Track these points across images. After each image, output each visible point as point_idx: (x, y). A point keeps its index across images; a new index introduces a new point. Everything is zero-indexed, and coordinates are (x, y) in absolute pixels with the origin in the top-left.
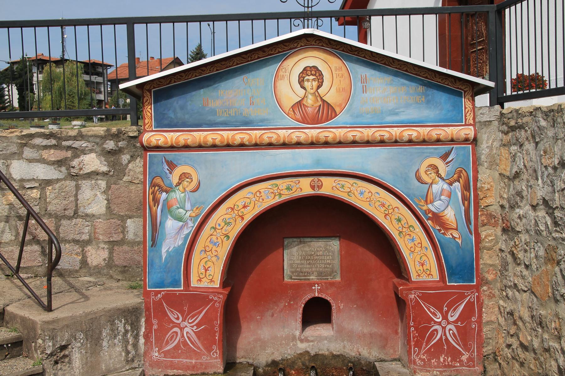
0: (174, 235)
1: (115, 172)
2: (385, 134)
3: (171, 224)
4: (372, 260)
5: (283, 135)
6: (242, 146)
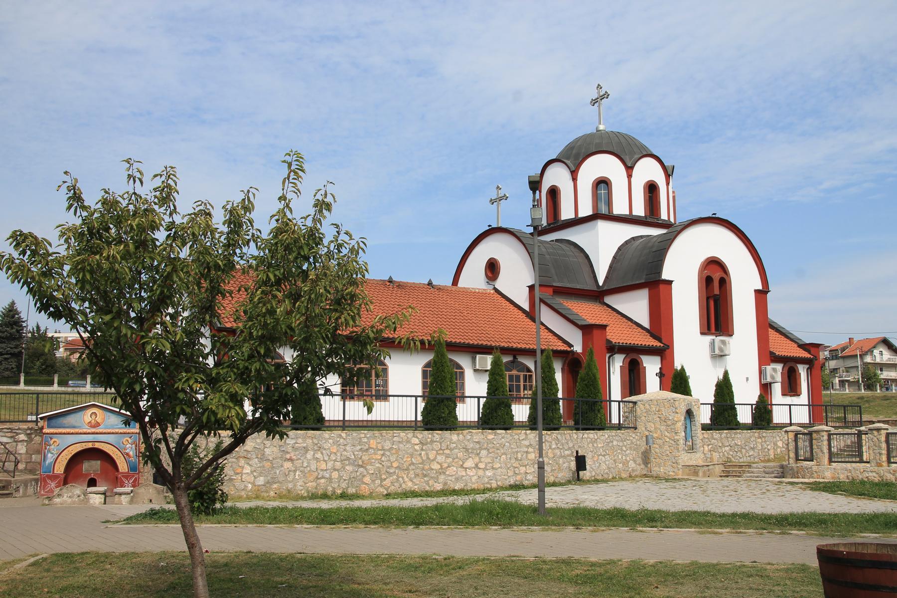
0: (50, 458)
1: (30, 440)
2: (113, 431)
3: (50, 455)
4: (109, 466)
5: (85, 430)
6: (72, 434)
